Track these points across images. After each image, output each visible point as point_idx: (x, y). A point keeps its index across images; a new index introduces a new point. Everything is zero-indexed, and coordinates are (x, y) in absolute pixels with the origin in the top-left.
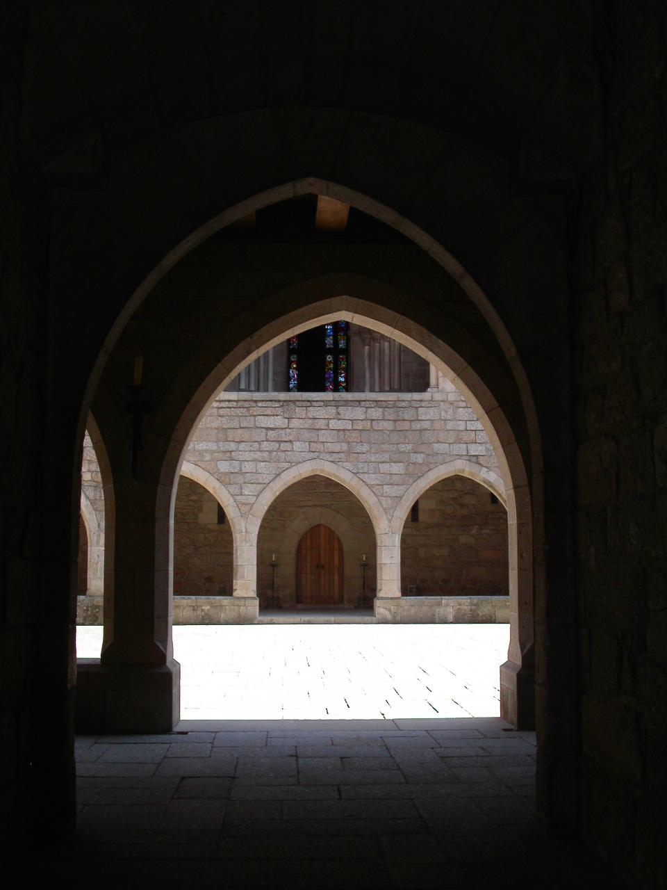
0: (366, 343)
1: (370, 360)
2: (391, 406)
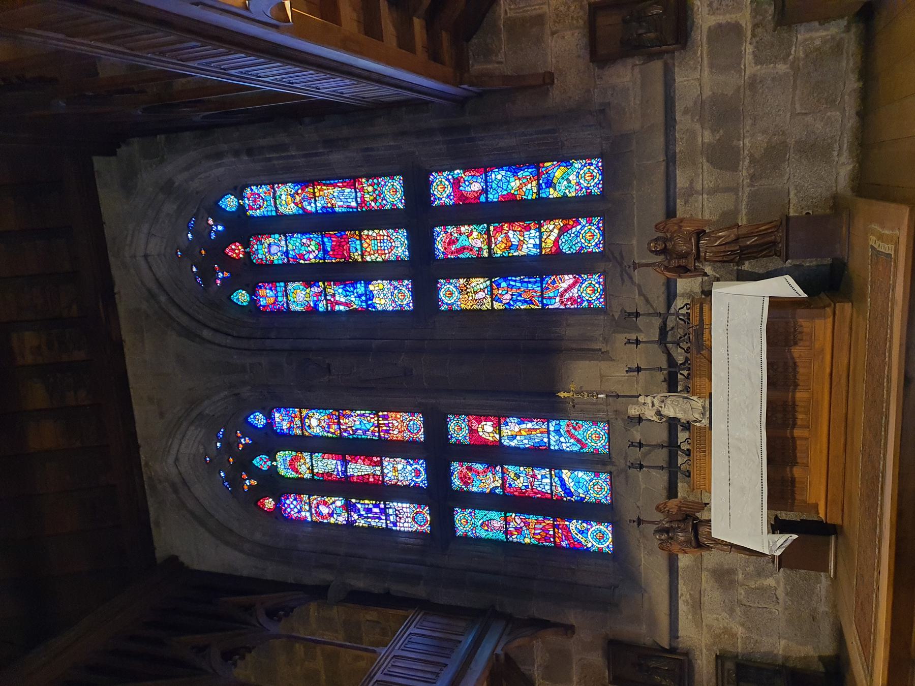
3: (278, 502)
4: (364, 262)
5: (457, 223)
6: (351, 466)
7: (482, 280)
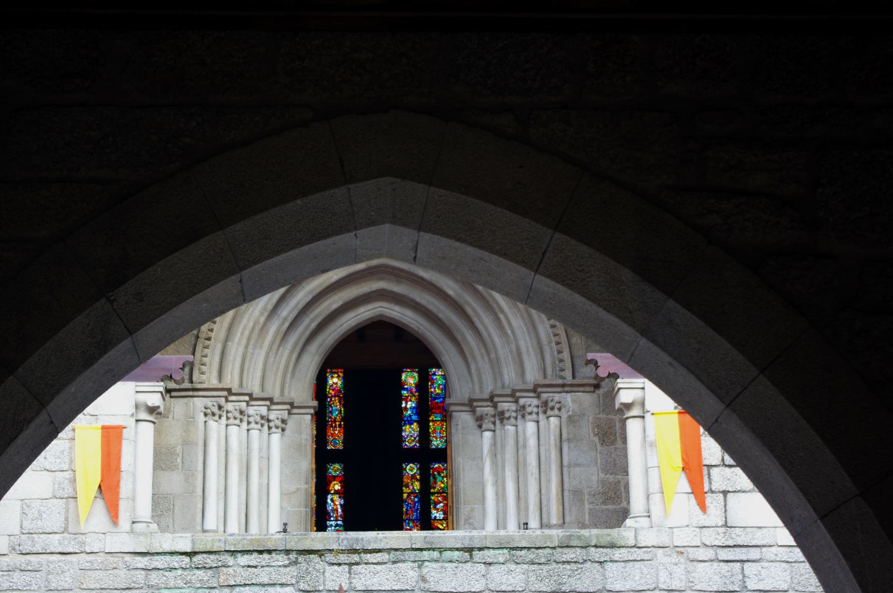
0: (484, 426)
1: (494, 463)
2: (543, 560)
4: (429, 421)
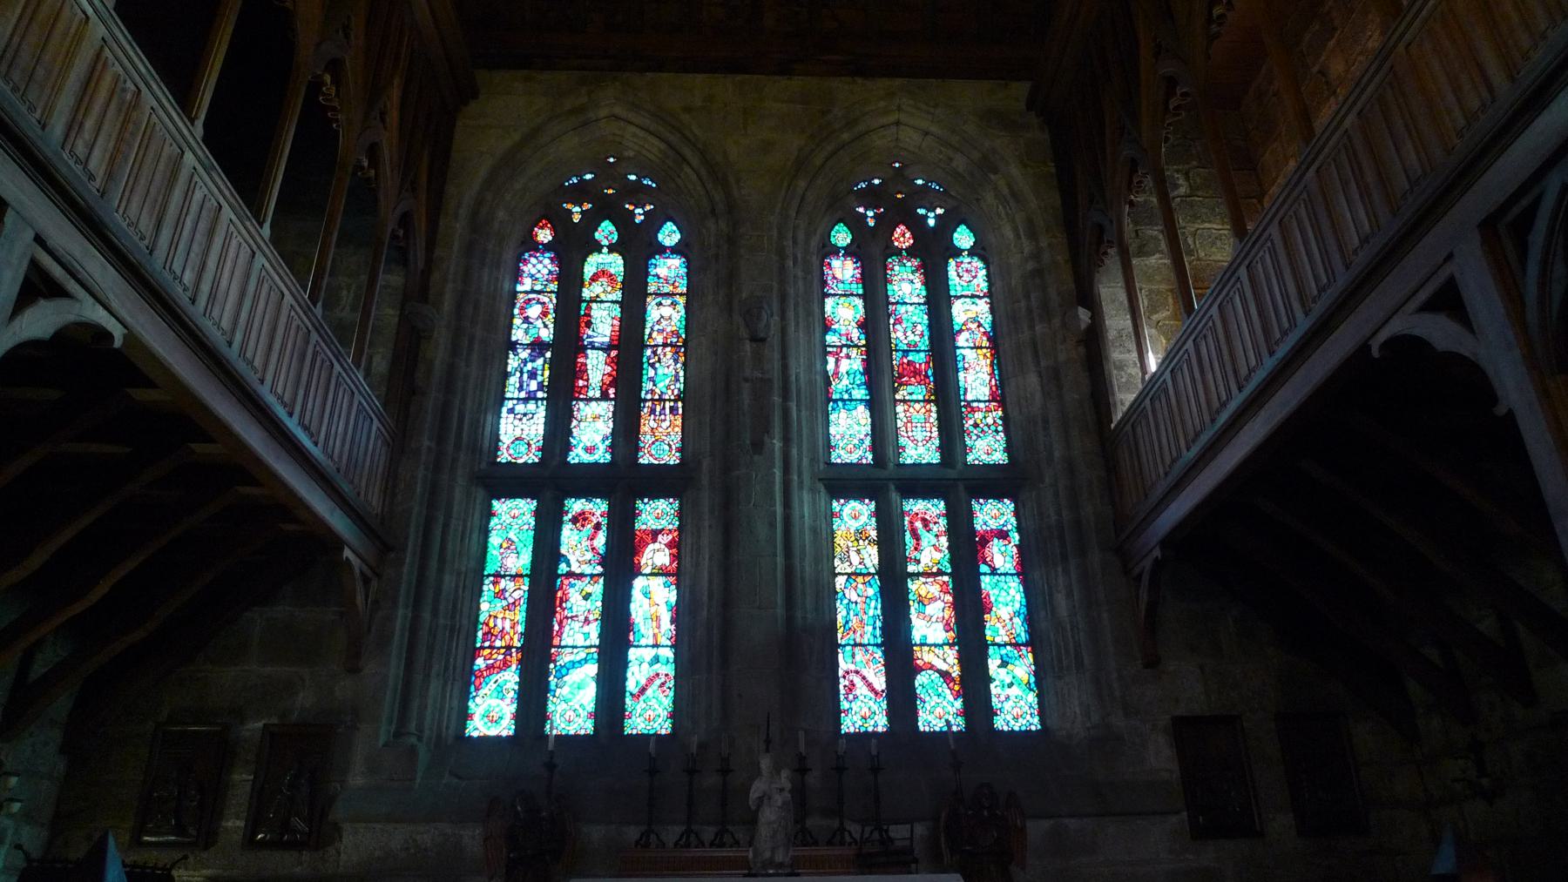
3: (548, 247)
5: (951, 532)
6: (602, 356)
7: (876, 561)
